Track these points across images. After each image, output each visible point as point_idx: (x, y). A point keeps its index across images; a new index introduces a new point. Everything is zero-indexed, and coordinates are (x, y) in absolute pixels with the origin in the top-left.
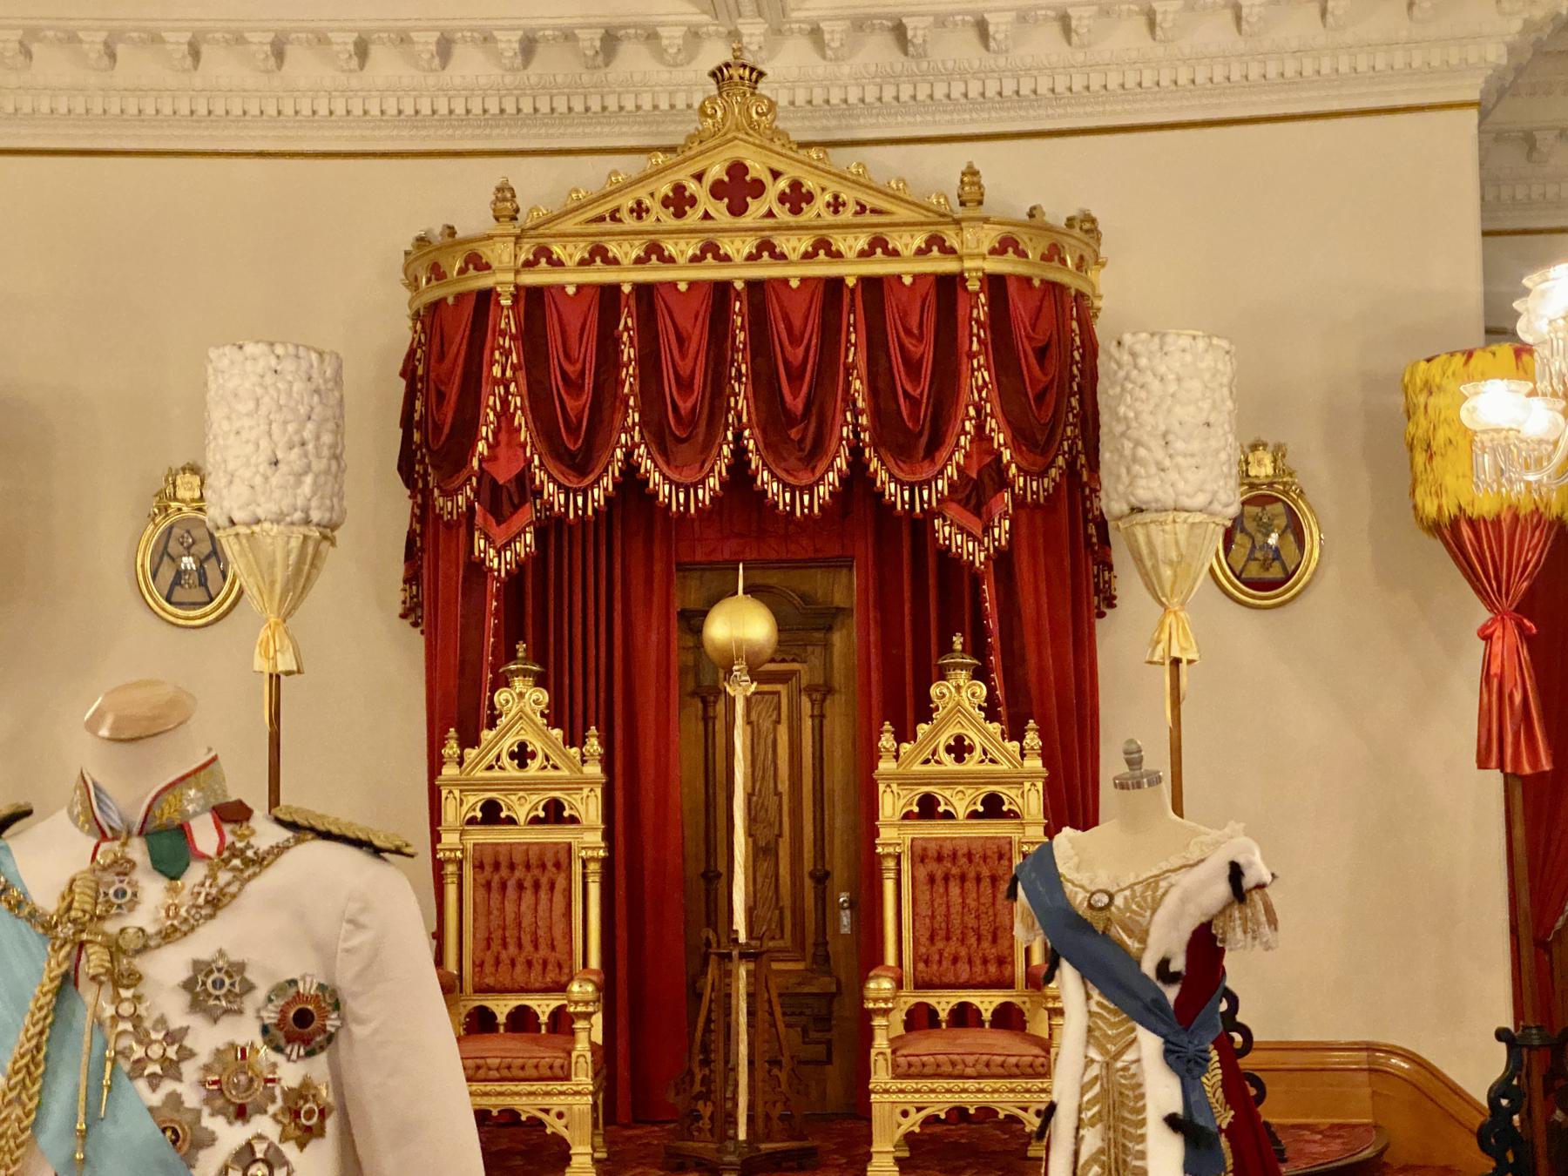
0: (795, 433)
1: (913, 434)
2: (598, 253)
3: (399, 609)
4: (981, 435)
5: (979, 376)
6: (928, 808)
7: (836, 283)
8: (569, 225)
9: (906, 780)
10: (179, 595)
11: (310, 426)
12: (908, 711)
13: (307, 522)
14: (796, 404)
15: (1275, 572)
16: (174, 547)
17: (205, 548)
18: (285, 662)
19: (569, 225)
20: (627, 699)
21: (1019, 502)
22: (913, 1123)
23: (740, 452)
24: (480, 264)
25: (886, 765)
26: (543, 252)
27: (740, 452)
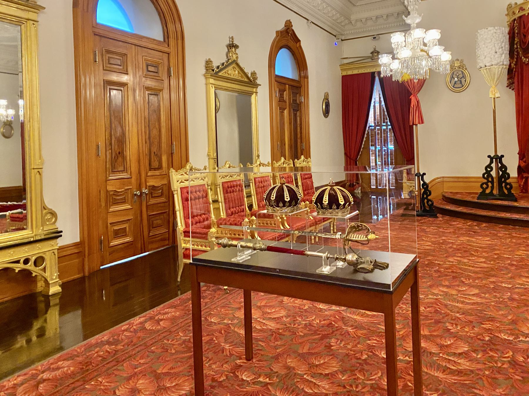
3: (506, 85)
10: (456, 86)
11: (503, 44)
13: (503, 65)
16: (454, 76)
17: (461, 76)
18: (497, 95)
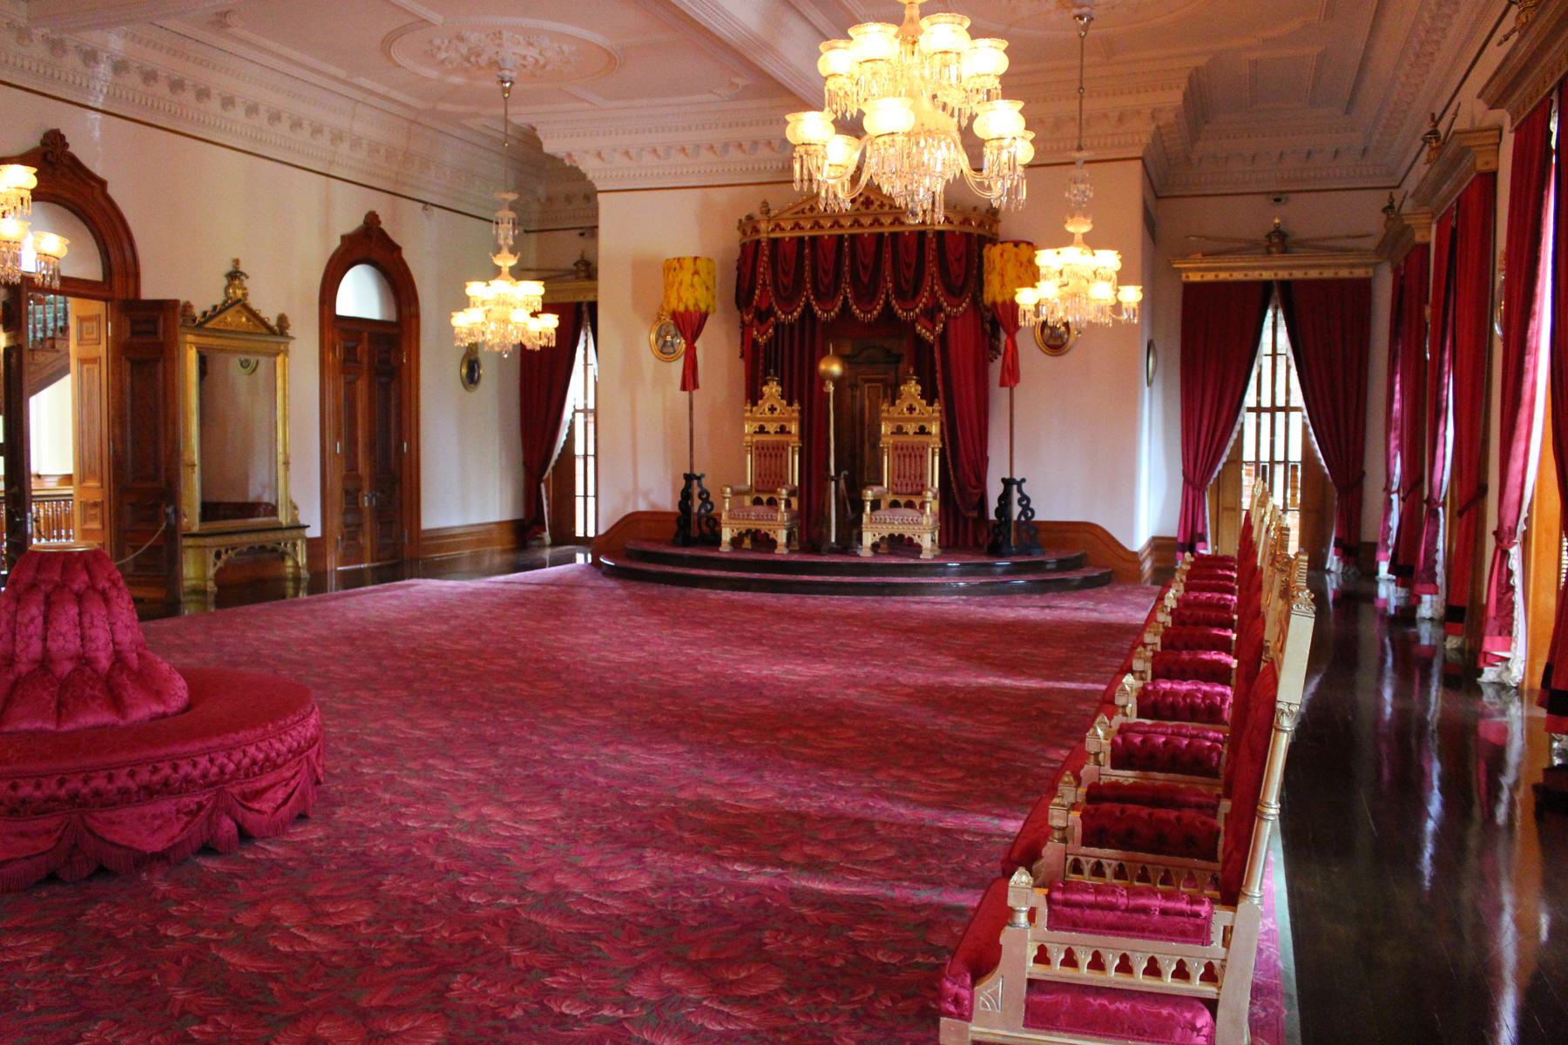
0: (866, 295)
1: (908, 293)
2: (797, 226)
4: (933, 292)
5: (932, 269)
6: (899, 431)
7: (881, 235)
8: (787, 215)
9: (891, 420)
12: (894, 396)
14: (865, 280)
15: (1059, 343)
19: (787, 215)
20: (804, 389)
21: (947, 317)
22: (877, 539)
23: (846, 298)
24: (756, 230)
25: (884, 415)
26: (778, 225)
27: (846, 298)
